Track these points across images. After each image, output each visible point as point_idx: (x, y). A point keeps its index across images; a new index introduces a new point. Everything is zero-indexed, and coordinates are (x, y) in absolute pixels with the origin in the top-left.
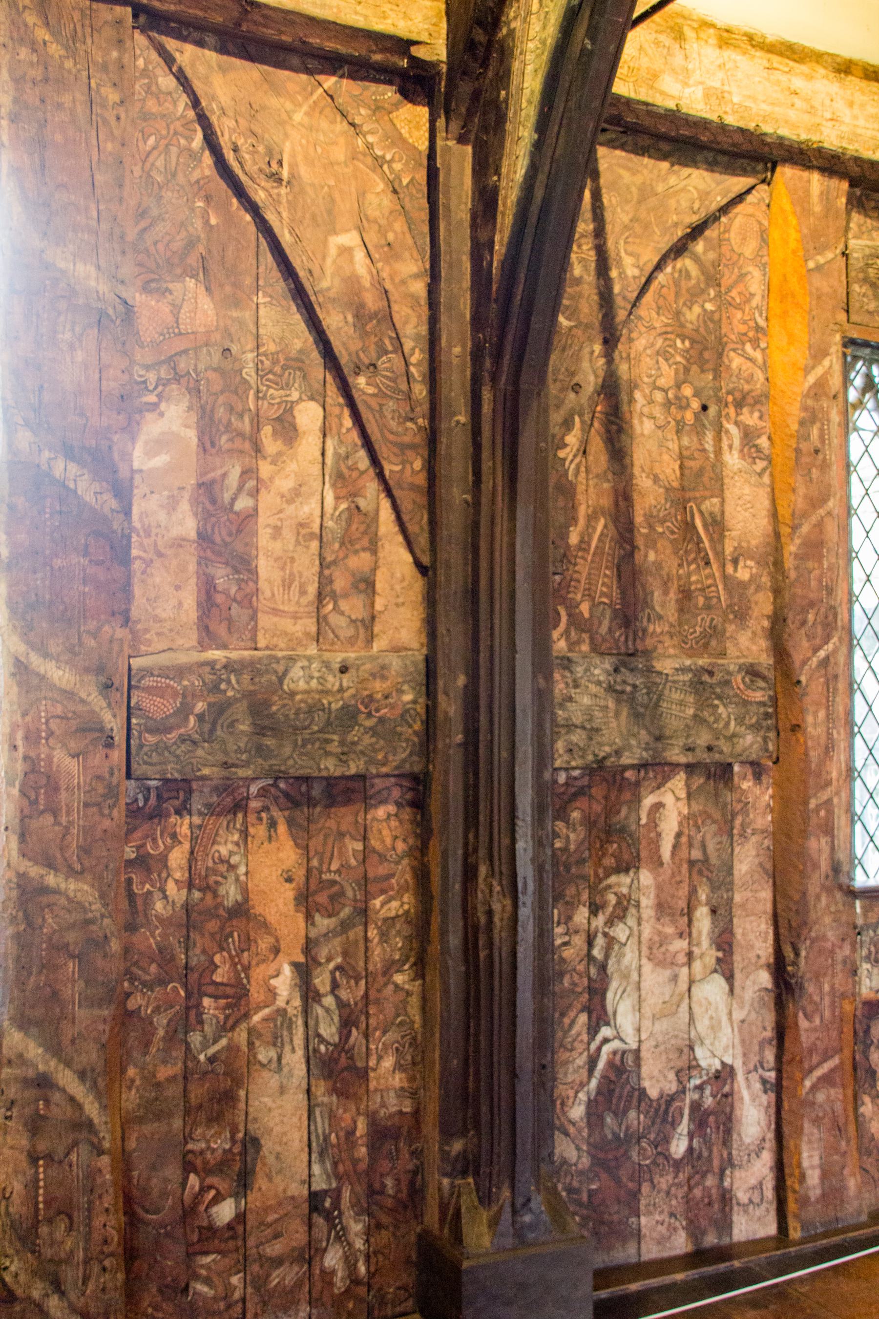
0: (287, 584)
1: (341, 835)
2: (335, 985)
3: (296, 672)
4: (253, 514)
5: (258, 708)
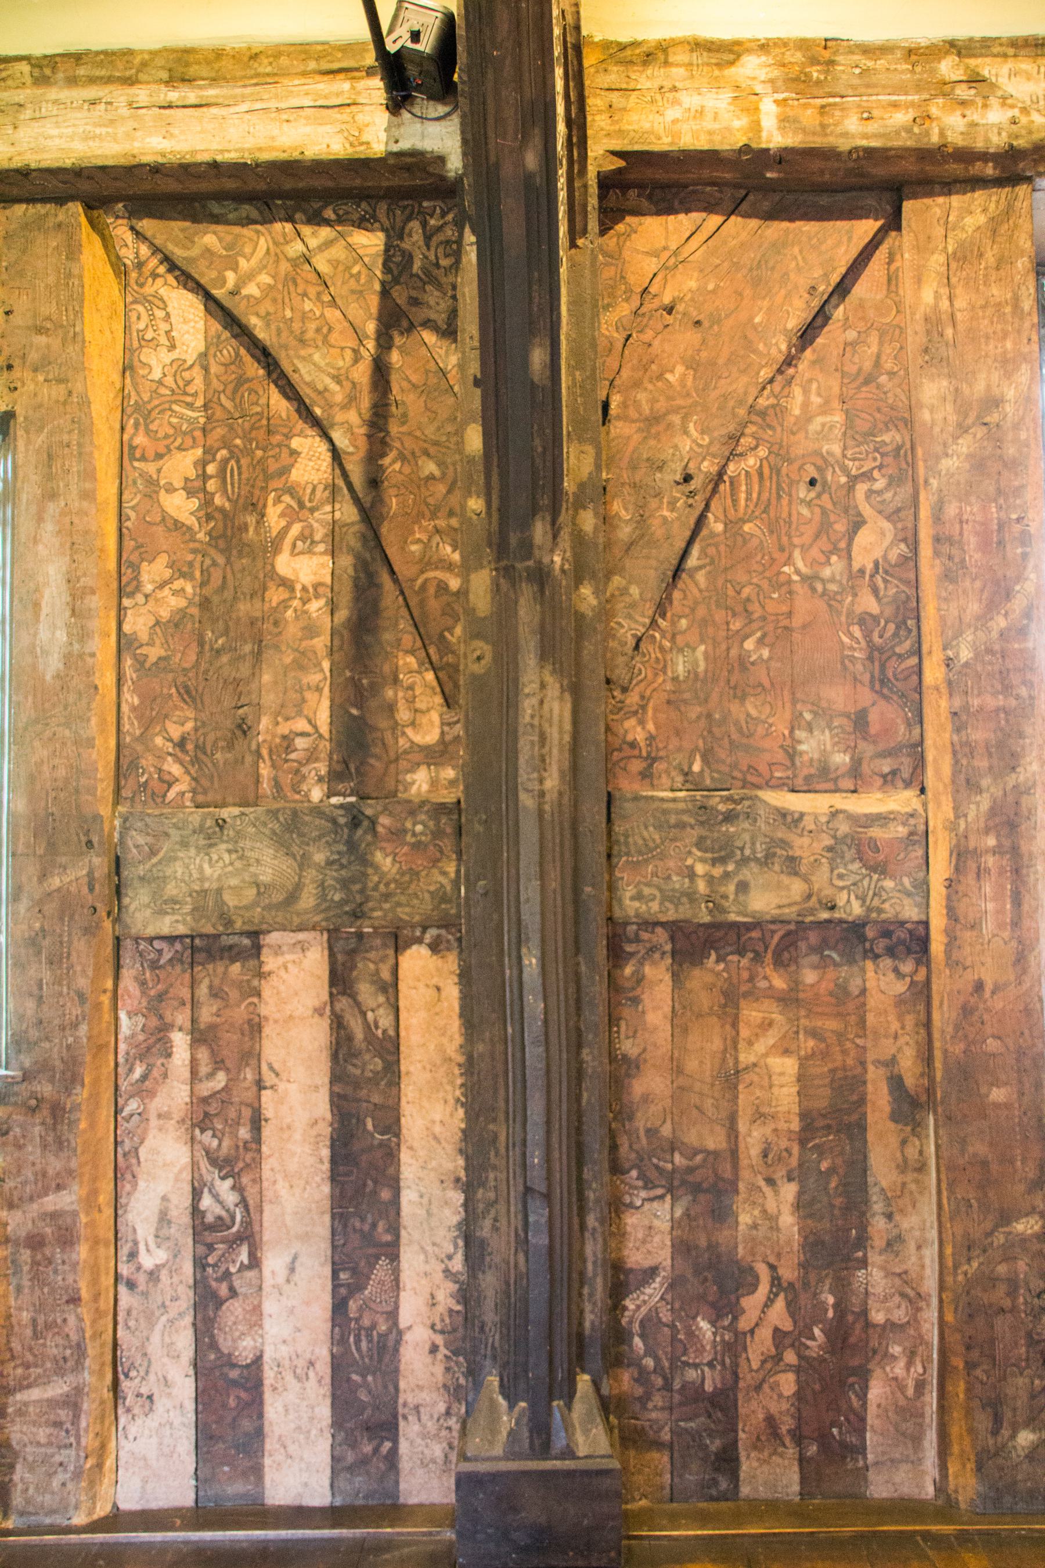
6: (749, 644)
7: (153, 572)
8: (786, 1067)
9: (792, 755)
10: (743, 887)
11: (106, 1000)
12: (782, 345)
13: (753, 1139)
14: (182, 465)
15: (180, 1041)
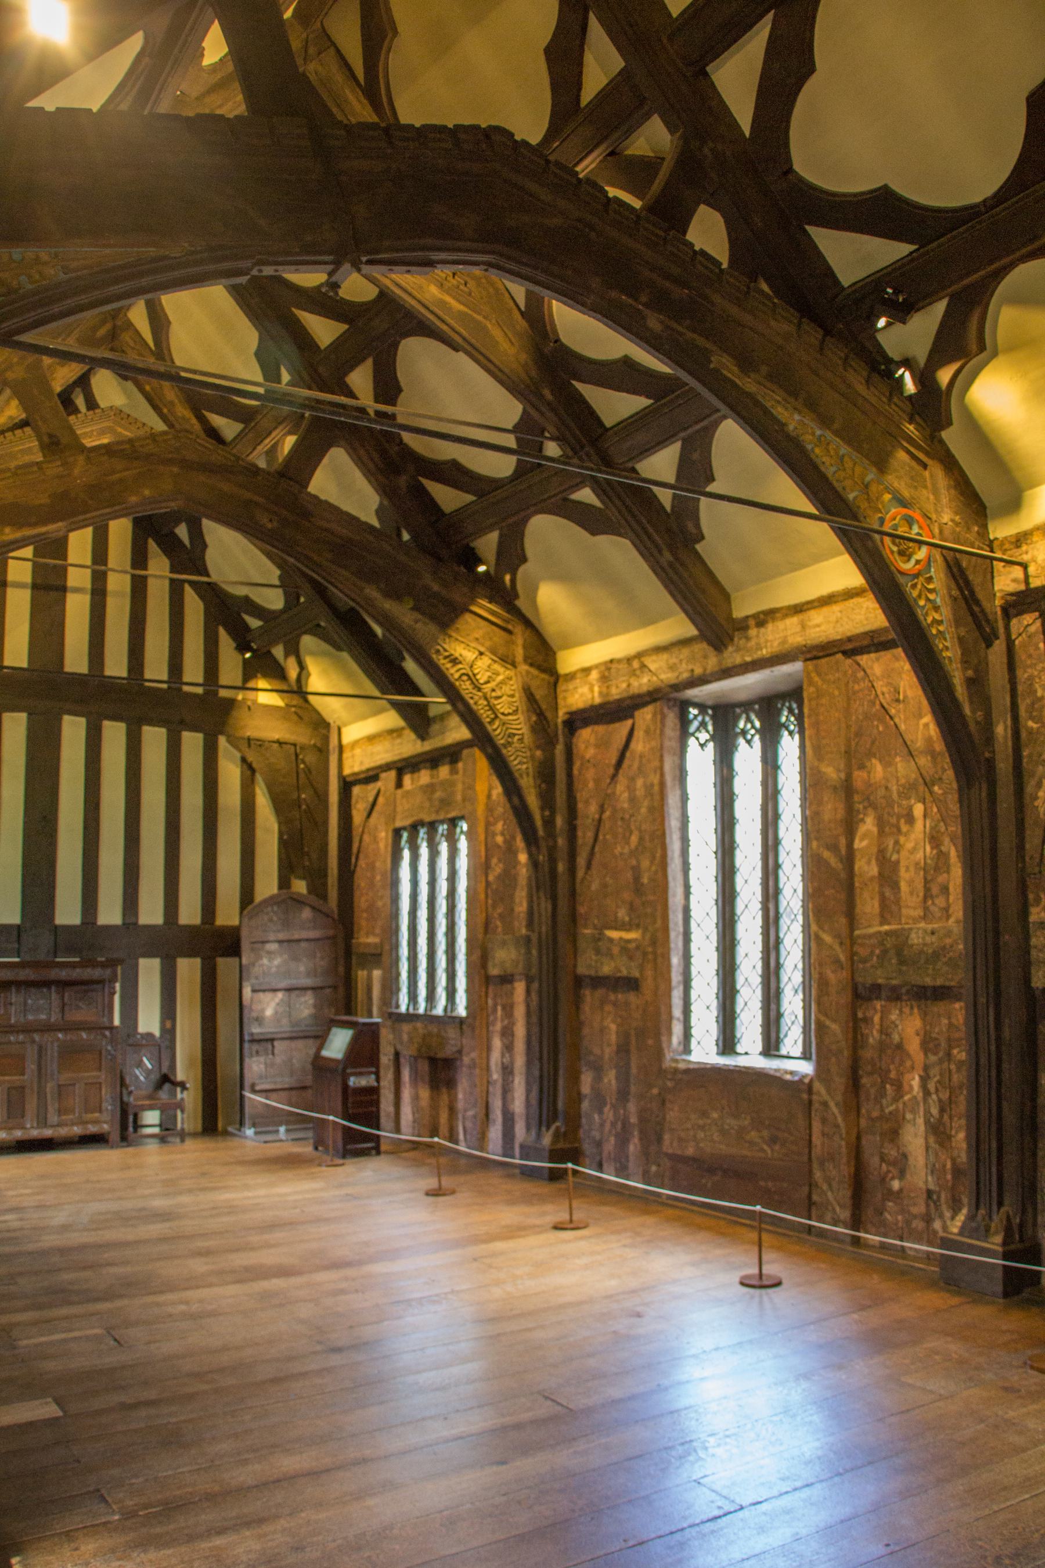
0: (911, 893)
1: (939, 1016)
2: (937, 1090)
3: (913, 935)
4: (898, 862)
5: (899, 953)
6: (608, 879)
7: (494, 861)
8: (613, 1027)
9: (616, 917)
10: (602, 964)
11: (483, 994)
12: (611, 771)
13: (607, 1051)
14: (499, 826)
15: (499, 1008)
